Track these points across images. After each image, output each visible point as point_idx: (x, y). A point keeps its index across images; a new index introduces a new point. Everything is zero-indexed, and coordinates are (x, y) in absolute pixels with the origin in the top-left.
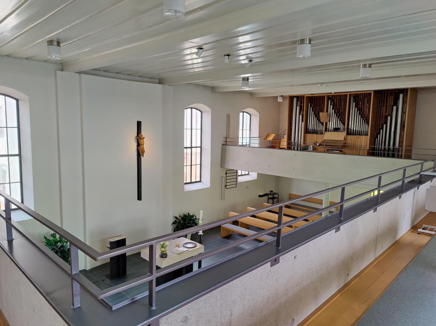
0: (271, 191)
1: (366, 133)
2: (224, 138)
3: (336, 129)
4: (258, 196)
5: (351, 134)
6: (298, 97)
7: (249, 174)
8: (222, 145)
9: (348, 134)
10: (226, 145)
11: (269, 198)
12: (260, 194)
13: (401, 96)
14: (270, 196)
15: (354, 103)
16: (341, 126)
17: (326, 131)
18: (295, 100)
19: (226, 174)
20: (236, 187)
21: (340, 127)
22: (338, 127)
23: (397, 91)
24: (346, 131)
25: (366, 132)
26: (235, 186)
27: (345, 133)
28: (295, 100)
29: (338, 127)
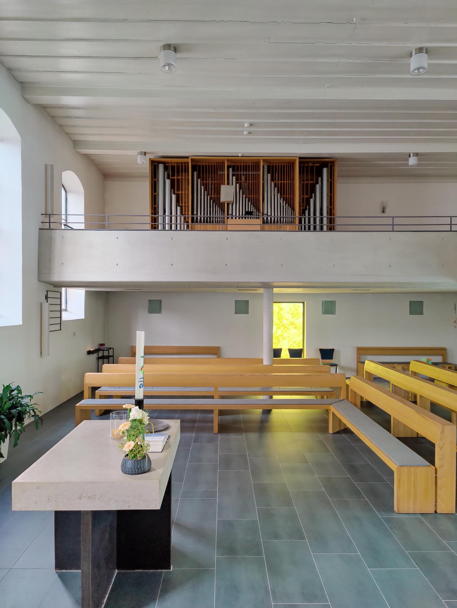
0: (102, 345)
1: (290, 221)
2: (42, 214)
3: (249, 213)
4: (86, 353)
5: (267, 222)
6: (167, 165)
7: (68, 309)
8: (40, 229)
9: (264, 222)
10: (50, 229)
11: (99, 358)
12: (88, 350)
13: (325, 170)
14: (101, 354)
15: (269, 175)
16: (253, 209)
17: (228, 218)
18: (161, 168)
19: (47, 297)
20: (61, 329)
21: (252, 211)
22: (250, 210)
23: (318, 165)
24: (261, 218)
25: (290, 219)
26: (58, 327)
27: (259, 221)
28: (161, 168)
29: (250, 210)
